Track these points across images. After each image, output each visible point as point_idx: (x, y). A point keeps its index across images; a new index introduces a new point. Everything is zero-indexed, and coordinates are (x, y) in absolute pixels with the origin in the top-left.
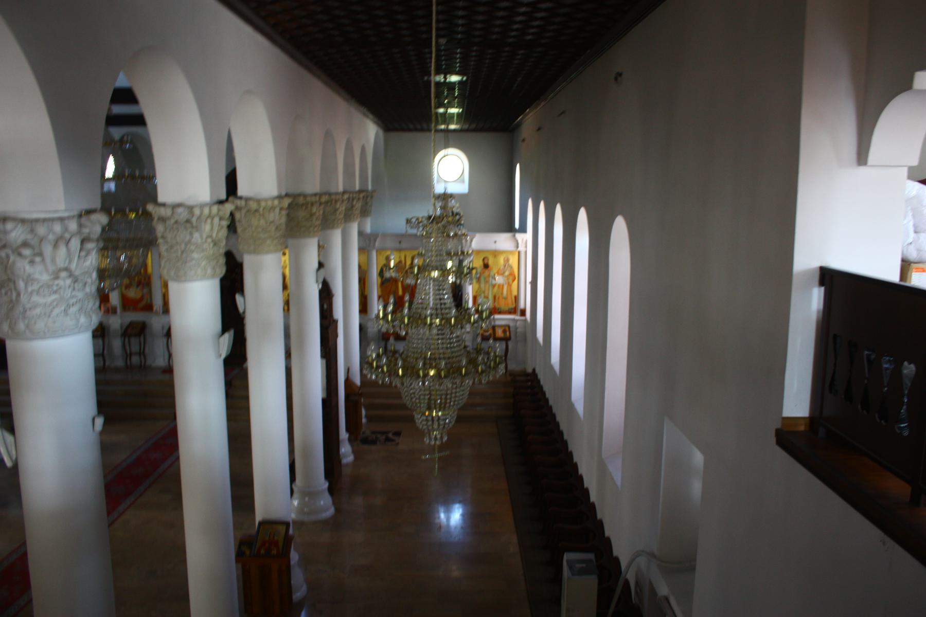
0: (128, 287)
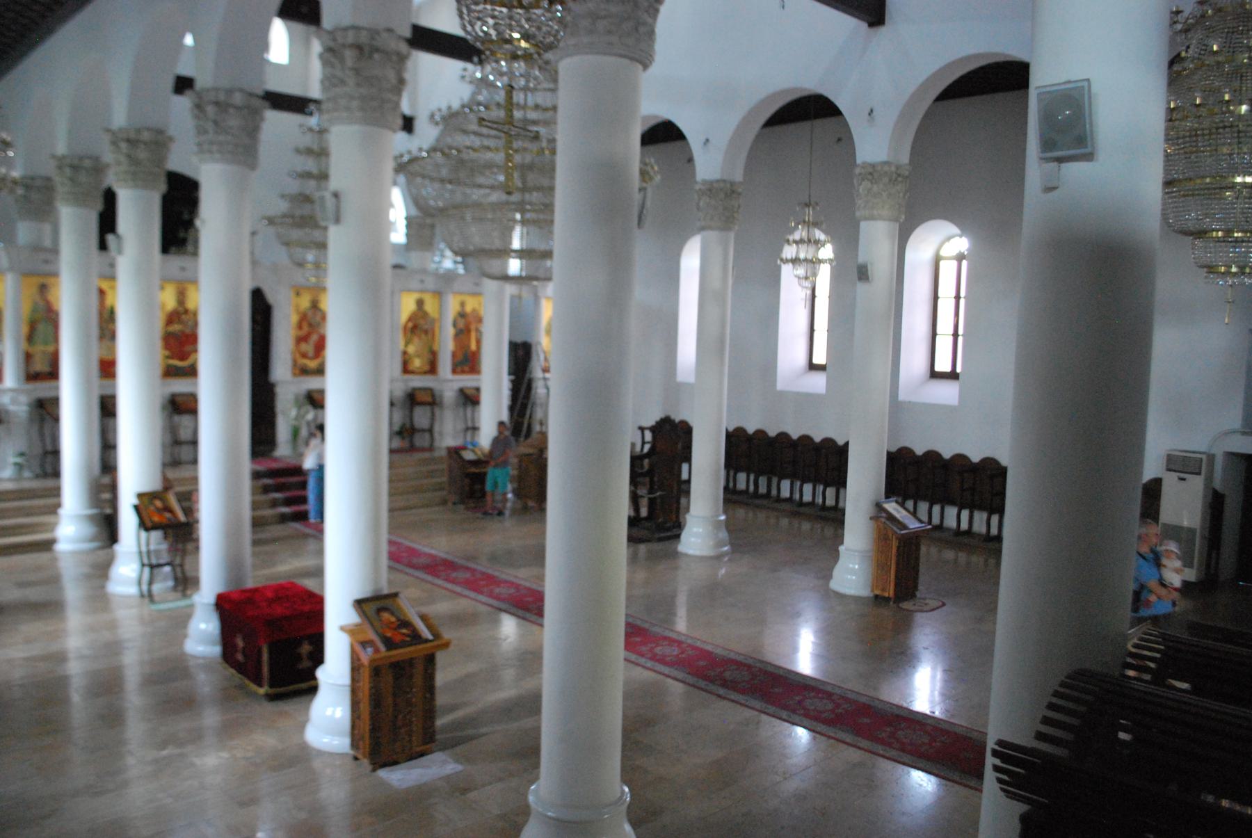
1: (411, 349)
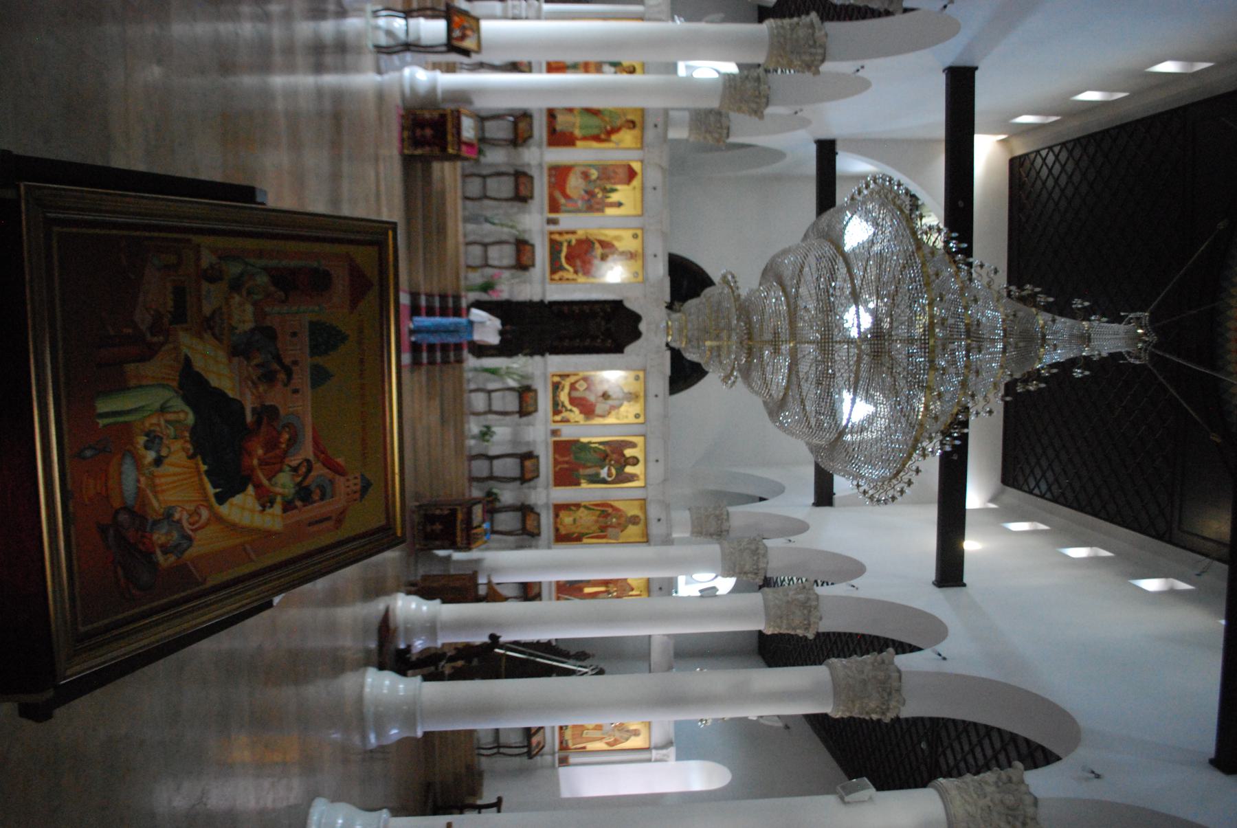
0: (586, 175)
1: (582, 513)
